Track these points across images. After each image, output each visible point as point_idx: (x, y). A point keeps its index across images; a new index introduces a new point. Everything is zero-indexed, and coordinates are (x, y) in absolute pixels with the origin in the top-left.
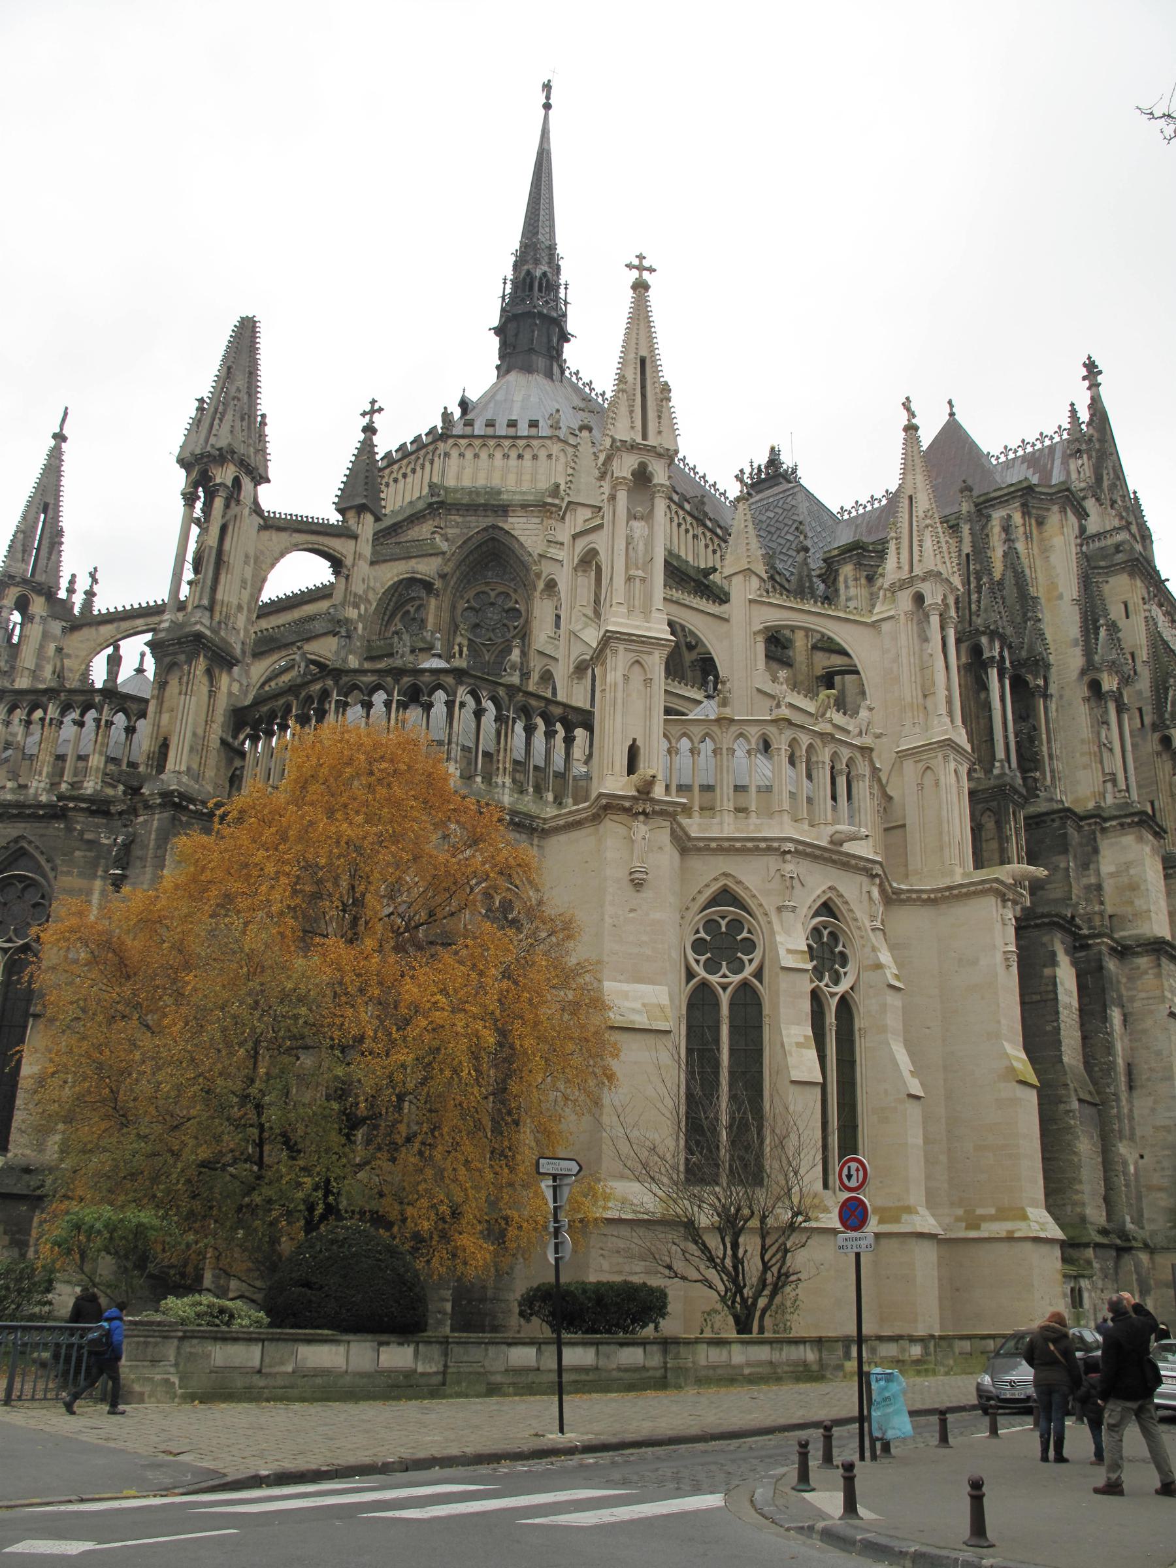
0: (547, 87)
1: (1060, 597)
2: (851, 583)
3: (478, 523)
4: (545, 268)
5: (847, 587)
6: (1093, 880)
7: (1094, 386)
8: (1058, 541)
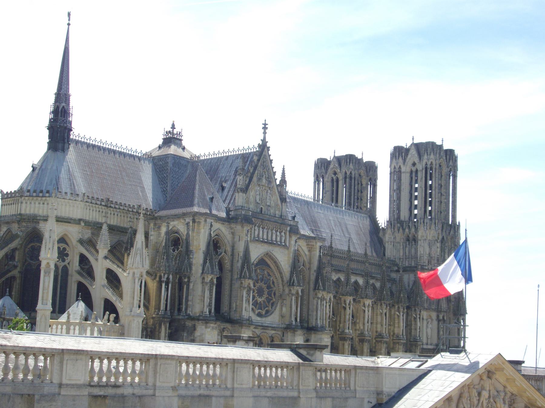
0: (69, 14)
1: (200, 249)
2: (152, 230)
3: (31, 225)
4: (64, 104)
5: (151, 231)
6: (192, 338)
7: (265, 133)
8: (202, 231)
